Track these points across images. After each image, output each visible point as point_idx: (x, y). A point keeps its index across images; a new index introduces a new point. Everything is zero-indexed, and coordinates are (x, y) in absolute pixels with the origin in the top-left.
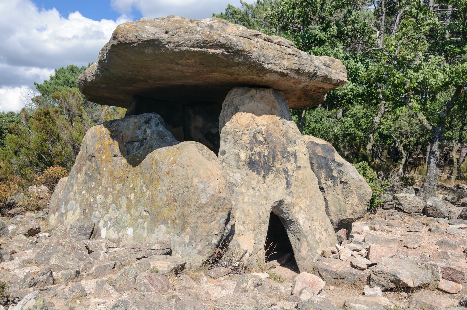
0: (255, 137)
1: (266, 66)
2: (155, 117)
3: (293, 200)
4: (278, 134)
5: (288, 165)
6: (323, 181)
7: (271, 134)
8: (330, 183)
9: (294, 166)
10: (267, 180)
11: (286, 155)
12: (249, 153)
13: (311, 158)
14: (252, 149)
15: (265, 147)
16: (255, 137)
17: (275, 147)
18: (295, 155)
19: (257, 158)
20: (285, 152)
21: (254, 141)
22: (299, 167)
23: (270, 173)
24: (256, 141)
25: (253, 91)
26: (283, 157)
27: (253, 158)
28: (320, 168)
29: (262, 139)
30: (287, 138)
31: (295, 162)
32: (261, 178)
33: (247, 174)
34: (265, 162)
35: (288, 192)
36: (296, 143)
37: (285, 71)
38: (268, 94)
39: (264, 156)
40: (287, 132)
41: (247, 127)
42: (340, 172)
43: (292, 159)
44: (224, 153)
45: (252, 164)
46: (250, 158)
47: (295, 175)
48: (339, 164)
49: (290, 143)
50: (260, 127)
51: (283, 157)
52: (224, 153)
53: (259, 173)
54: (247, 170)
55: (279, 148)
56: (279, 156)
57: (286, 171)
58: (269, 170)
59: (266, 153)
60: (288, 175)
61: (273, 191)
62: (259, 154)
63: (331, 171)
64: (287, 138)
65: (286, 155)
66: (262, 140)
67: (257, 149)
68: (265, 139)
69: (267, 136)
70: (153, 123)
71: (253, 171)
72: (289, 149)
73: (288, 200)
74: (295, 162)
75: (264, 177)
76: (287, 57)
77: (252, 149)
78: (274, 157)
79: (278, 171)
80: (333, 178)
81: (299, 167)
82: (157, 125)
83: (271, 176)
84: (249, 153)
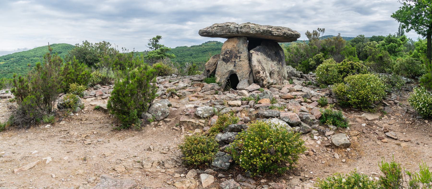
0: (226, 52)
5: (237, 60)
16: (226, 52)
18: (240, 57)
21: (226, 53)
26: (235, 57)
40: (238, 50)
43: (238, 58)
45: (224, 60)
57: (235, 62)
61: (230, 67)
62: (226, 57)
65: (236, 57)
73: (235, 70)
79: (232, 61)
83: (229, 63)
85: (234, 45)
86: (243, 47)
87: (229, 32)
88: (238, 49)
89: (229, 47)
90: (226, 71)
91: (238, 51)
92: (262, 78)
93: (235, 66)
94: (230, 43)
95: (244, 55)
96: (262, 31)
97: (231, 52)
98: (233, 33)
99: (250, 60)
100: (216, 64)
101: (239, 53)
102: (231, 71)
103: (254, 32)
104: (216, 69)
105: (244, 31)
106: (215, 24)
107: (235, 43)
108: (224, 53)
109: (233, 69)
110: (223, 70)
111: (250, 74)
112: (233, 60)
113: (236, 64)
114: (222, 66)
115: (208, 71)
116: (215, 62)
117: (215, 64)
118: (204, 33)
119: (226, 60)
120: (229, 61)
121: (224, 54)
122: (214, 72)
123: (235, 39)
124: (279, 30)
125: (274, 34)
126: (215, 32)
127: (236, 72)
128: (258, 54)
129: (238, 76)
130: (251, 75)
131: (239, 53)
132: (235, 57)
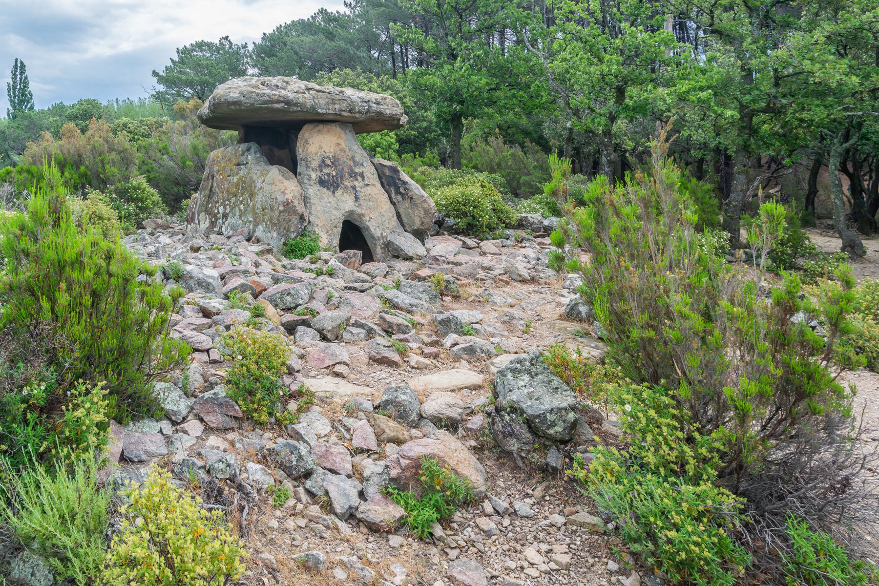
0: (323, 161)
2: (254, 146)
5: (356, 183)
6: (393, 195)
8: (399, 198)
9: (362, 183)
10: (336, 194)
11: (353, 175)
12: (319, 174)
13: (380, 178)
14: (321, 171)
16: (323, 161)
18: (362, 175)
21: (323, 164)
22: (367, 185)
25: (321, 127)
26: (351, 176)
28: (390, 185)
30: (354, 162)
31: (363, 180)
32: (330, 193)
38: (336, 129)
42: (405, 189)
43: (360, 179)
44: (300, 174)
45: (322, 183)
47: (364, 192)
48: (404, 183)
51: (351, 176)
52: (300, 174)
53: (328, 189)
54: (317, 187)
55: (346, 170)
56: (347, 176)
57: (354, 188)
58: (338, 187)
59: (334, 174)
62: (328, 174)
63: (399, 188)
64: (354, 162)
65: (353, 175)
67: (326, 171)
70: (252, 150)
72: (357, 170)
74: (363, 180)
75: (334, 192)
77: (321, 171)
78: (342, 178)
79: (346, 187)
80: (401, 193)
81: (367, 185)
82: (255, 152)
83: (339, 192)
84: (319, 174)
87: (350, 111)
93: (357, 199)
97: (335, 162)
105: (388, 111)
107: (339, 137)
113: (360, 195)
119: (329, 184)
121: (320, 166)
126: (312, 107)
131: (356, 164)
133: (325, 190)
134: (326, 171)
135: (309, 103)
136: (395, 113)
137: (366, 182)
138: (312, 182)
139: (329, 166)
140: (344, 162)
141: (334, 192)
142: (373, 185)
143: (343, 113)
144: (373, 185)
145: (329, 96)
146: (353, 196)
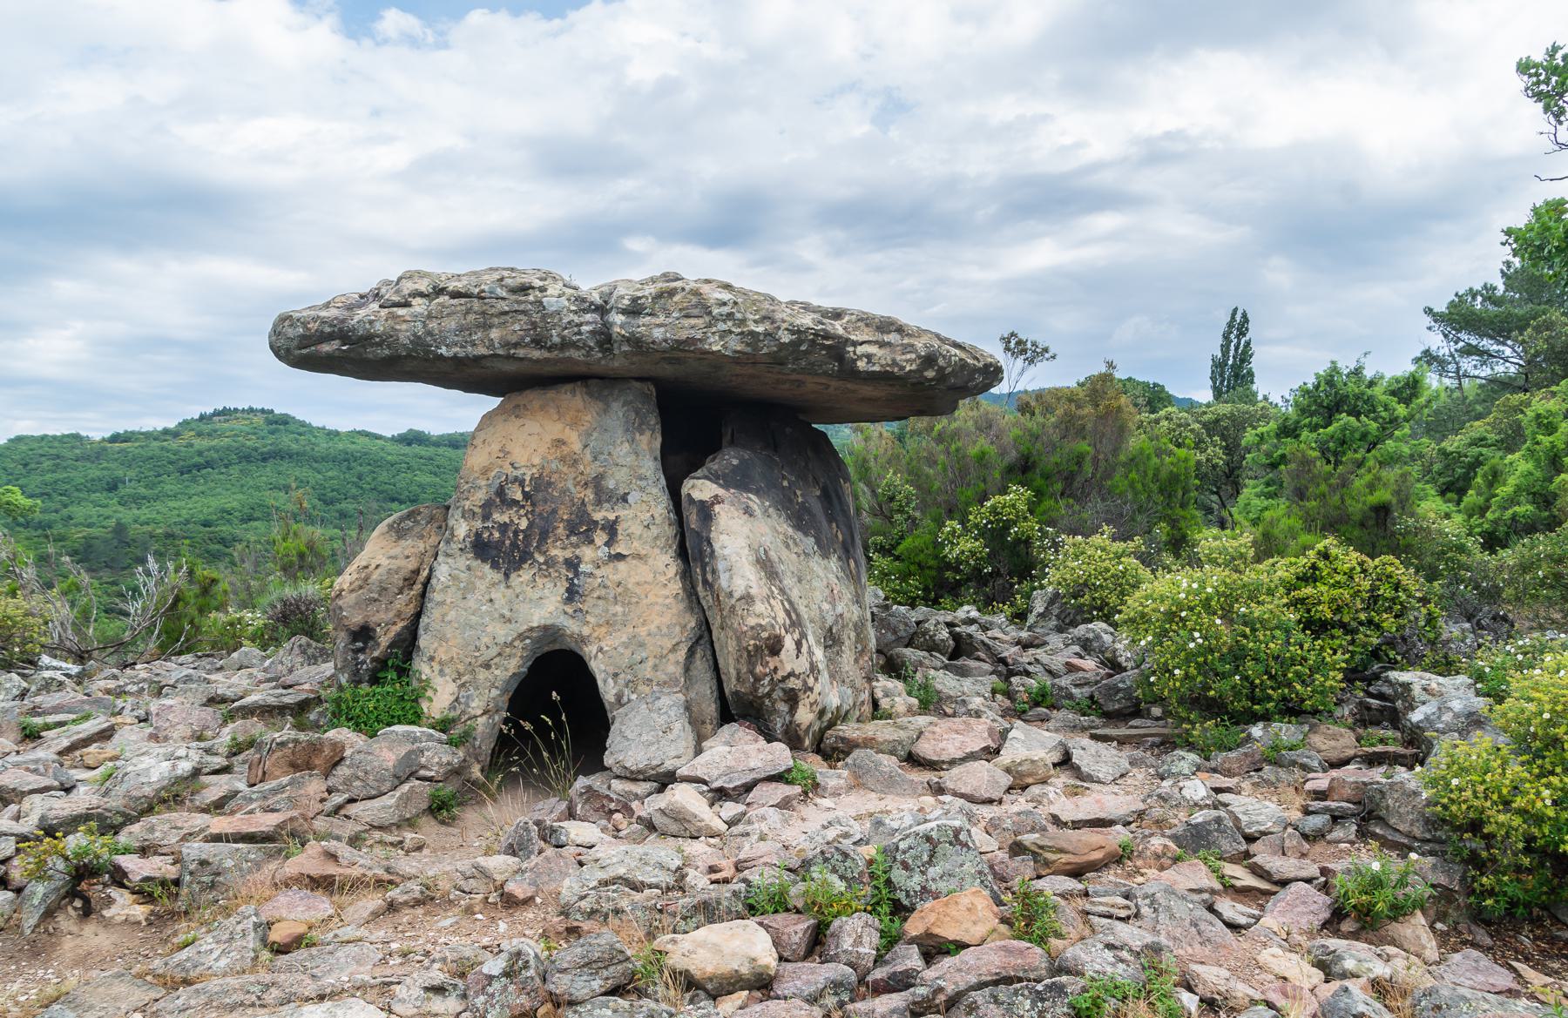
0: (501, 492)
1: (443, 351)
3: (586, 631)
4: (570, 485)
5: (587, 553)
7: (549, 484)
12: (479, 524)
14: (486, 517)
15: (522, 512)
16: (501, 492)
17: (554, 511)
18: (611, 529)
19: (497, 535)
20: (581, 523)
21: (500, 497)
22: (620, 557)
23: (526, 566)
24: (503, 501)
26: (572, 530)
27: (486, 535)
29: (519, 496)
31: (608, 544)
32: (498, 576)
33: (469, 568)
34: (514, 545)
35: (570, 611)
36: (626, 501)
37: (501, 352)
39: (516, 533)
41: (485, 471)
43: (600, 537)
45: (481, 548)
46: (478, 535)
49: (608, 501)
50: (518, 473)
56: (561, 530)
57: (573, 564)
58: (523, 560)
59: (524, 524)
60: (577, 574)
61: (538, 603)
62: (503, 527)
65: (582, 528)
66: (519, 496)
67: (500, 517)
68: (526, 496)
69: (536, 489)
71: (484, 561)
72: (598, 516)
73: (572, 627)
75: (507, 576)
76: (496, 320)
77: (486, 517)
78: (544, 536)
81: (620, 557)
83: (526, 574)
85: (559, 443)
86: (630, 456)
87: (538, 342)
88: (591, 470)
89: (520, 455)
90: (504, 633)
91: (597, 482)
92: (793, 683)
93: (572, 594)
94: (532, 426)
95: (644, 514)
96: (786, 338)
98: (565, 344)
99: (692, 549)
100: (419, 585)
101: (604, 496)
102: (546, 628)
103: (735, 344)
104: (418, 615)
105: (658, 334)
106: (409, 276)
107: (574, 424)
108: (480, 496)
109: (563, 621)
110: (479, 631)
111: (691, 652)
112: (558, 553)
113: (585, 584)
114: (471, 602)
115: (364, 634)
116: (412, 565)
117: (409, 581)
118: (324, 338)
119: (500, 553)
120: (526, 556)
121: (487, 508)
122: (408, 643)
123: (573, 399)
124: (892, 337)
125: (862, 365)
126: (417, 340)
127: (583, 640)
128: (748, 512)
129: (597, 666)
130: (701, 666)
131: (604, 496)
132: (572, 530)
133: (487, 567)
134: (500, 517)
135: (405, 333)
136: (683, 335)
137: (619, 548)
138: (455, 546)
139: (516, 502)
140: (564, 491)
141: (507, 576)
142: (639, 557)
143: (521, 352)
144: (639, 557)
145: (476, 304)
146: (561, 588)
